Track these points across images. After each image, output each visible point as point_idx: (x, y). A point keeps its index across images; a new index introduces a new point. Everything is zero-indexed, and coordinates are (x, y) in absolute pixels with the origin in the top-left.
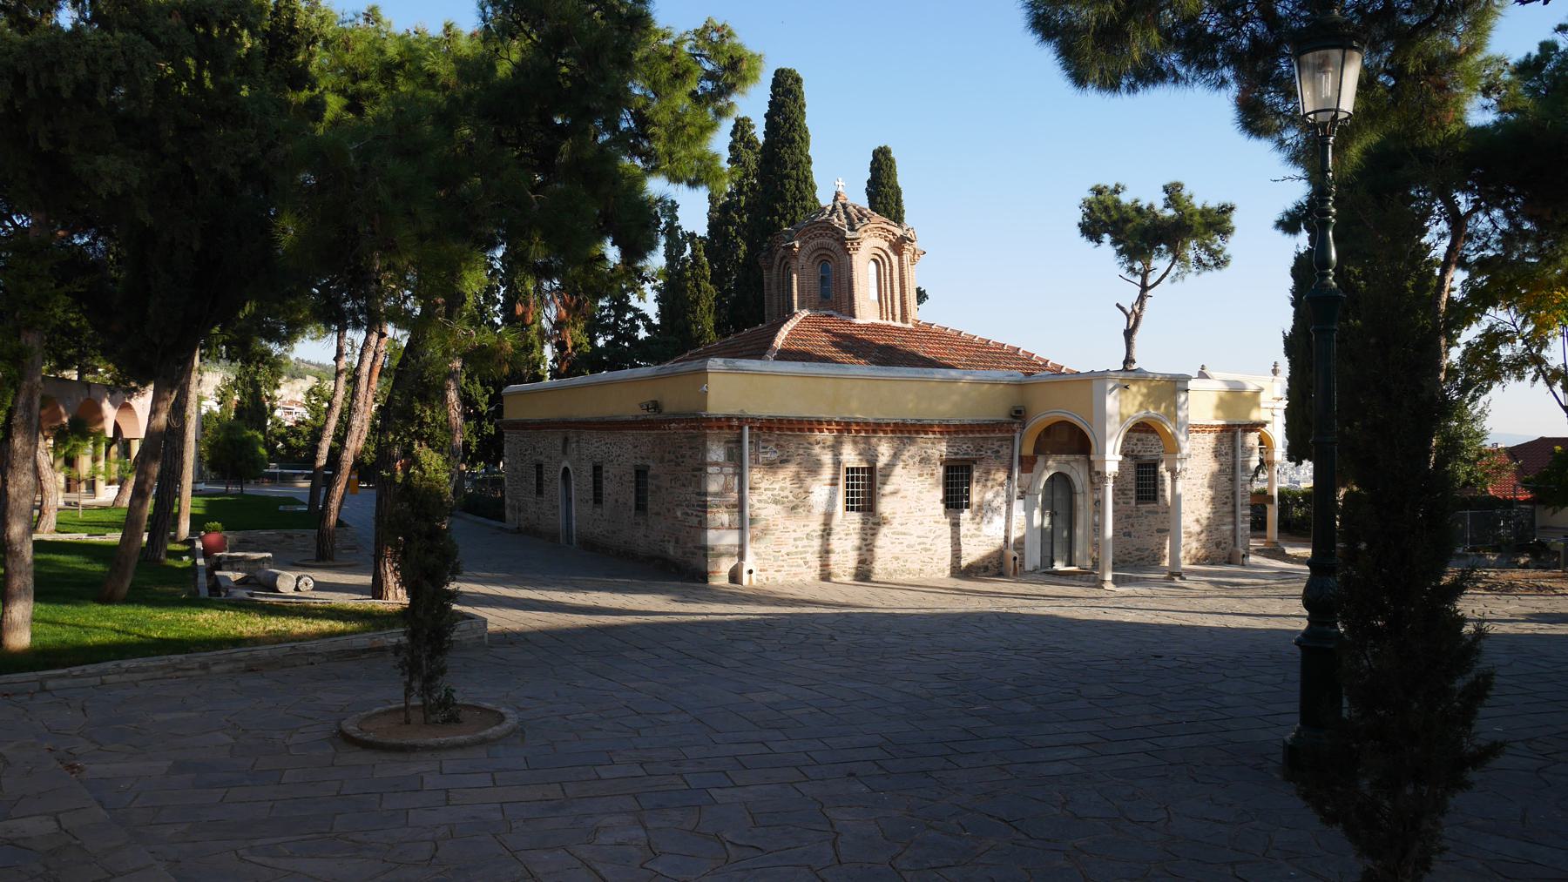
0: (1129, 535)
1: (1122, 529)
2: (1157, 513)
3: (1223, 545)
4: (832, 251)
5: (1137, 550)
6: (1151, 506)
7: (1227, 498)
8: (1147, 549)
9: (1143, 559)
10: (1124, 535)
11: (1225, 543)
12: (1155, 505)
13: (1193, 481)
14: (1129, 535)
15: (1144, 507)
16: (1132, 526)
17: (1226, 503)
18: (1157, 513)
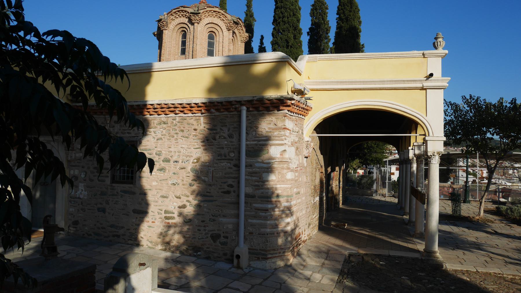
0: (104, 211)
1: (96, 205)
2: (134, 193)
3: (222, 239)
4: (190, 29)
5: (112, 226)
6: (127, 187)
7: (231, 186)
8: (123, 227)
9: (118, 236)
10: (99, 210)
11: (227, 237)
12: (132, 185)
13: (180, 165)
14: (104, 211)
15: (119, 187)
16: (108, 203)
17: (228, 192)
18: (134, 193)
